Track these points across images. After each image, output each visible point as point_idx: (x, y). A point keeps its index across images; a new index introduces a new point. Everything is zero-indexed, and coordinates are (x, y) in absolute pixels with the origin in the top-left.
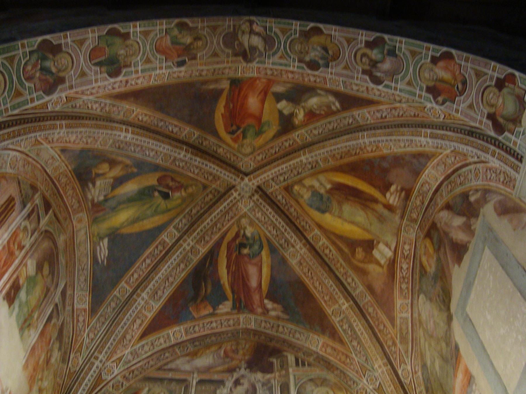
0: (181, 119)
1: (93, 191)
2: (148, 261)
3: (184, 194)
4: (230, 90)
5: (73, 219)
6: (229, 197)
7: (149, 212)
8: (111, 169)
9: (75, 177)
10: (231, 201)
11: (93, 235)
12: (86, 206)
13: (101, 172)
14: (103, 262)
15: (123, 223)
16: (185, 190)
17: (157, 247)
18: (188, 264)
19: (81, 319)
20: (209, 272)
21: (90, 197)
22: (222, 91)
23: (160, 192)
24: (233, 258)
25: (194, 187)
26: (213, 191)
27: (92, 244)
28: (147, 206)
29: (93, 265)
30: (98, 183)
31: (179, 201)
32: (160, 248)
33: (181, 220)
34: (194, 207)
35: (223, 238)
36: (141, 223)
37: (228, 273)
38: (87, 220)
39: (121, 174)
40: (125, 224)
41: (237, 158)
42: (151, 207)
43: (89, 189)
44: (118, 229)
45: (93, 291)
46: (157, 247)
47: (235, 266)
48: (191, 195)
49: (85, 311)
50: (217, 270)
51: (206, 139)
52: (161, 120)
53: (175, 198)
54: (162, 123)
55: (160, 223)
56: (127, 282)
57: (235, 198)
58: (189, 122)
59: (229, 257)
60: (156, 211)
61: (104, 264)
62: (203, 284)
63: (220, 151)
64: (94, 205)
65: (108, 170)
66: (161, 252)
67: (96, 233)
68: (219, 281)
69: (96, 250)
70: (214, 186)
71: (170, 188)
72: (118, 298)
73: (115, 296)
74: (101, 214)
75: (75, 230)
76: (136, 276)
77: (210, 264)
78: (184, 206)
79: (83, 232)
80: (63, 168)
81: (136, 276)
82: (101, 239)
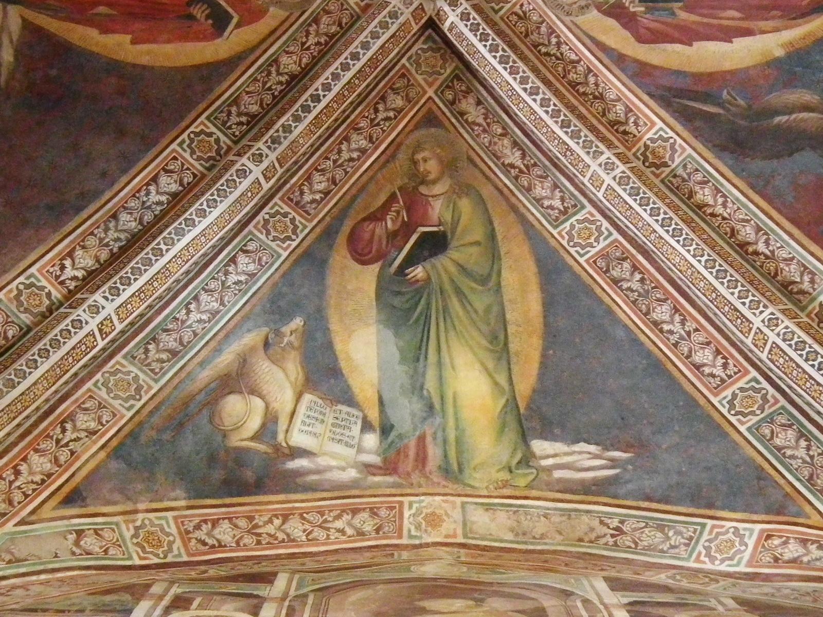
0: (127, 163)
1: (322, 461)
2: (662, 313)
3: (438, 189)
4: (30, 5)
5: (417, 542)
6: (460, 35)
7: (480, 301)
8: (254, 391)
9: (228, 501)
10: (474, 29)
11: (506, 484)
12: (388, 491)
13: (254, 423)
14: (614, 463)
15: (496, 384)
16: (423, 182)
17: (616, 282)
18: (699, 177)
19: (793, 550)
20: (741, 102)
21: (352, 474)
22: (28, 27)
23: (411, 261)
24: (694, 18)
25: (426, 154)
26: (449, 95)
27: (534, 493)
28: (455, 304)
29: (615, 497)
30: (298, 439)
31: (465, 205)
32: (622, 271)
33: (538, 201)
34: (496, 156)
35: (619, 60)
36: (511, 329)
37: (748, 33)
38: (438, 498)
39: (294, 368)
40: (502, 380)
41: (328, 12)
42: (459, 292)
43: (318, 472)
44: (512, 402)
45: (711, 506)
46: (616, 282)
47: (724, 9)
48: (450, 166)
49: (769, 537)
50: (732, 73)
51: (236, 102)
52: (115, 216)
53: (448, 217)
54: (124, 217)
55: (530, 268)
56: (716, 390)
57: (465, 17)
58: (148, 142)
59: (688, 36)
60: (483, 280)
61: (628, 461)
62: (784, 118)
63: (289, 64)
64: (389, 466)
65: (258, 403)
66: (635, 268)
67: (505, 475)
68: (774, 64)
69: (559, 480)
70: (430, 93)
71: (407, 229)
72: (770, 419)
73: (755, 429)
74: (434, 453)
75: (460, 540)
76: (704, 356)
77: (706, 97)
78: (487, 191)
79: (480, 519)
80: (169, 523)
81: (704, 356)
82: (527, 459)
